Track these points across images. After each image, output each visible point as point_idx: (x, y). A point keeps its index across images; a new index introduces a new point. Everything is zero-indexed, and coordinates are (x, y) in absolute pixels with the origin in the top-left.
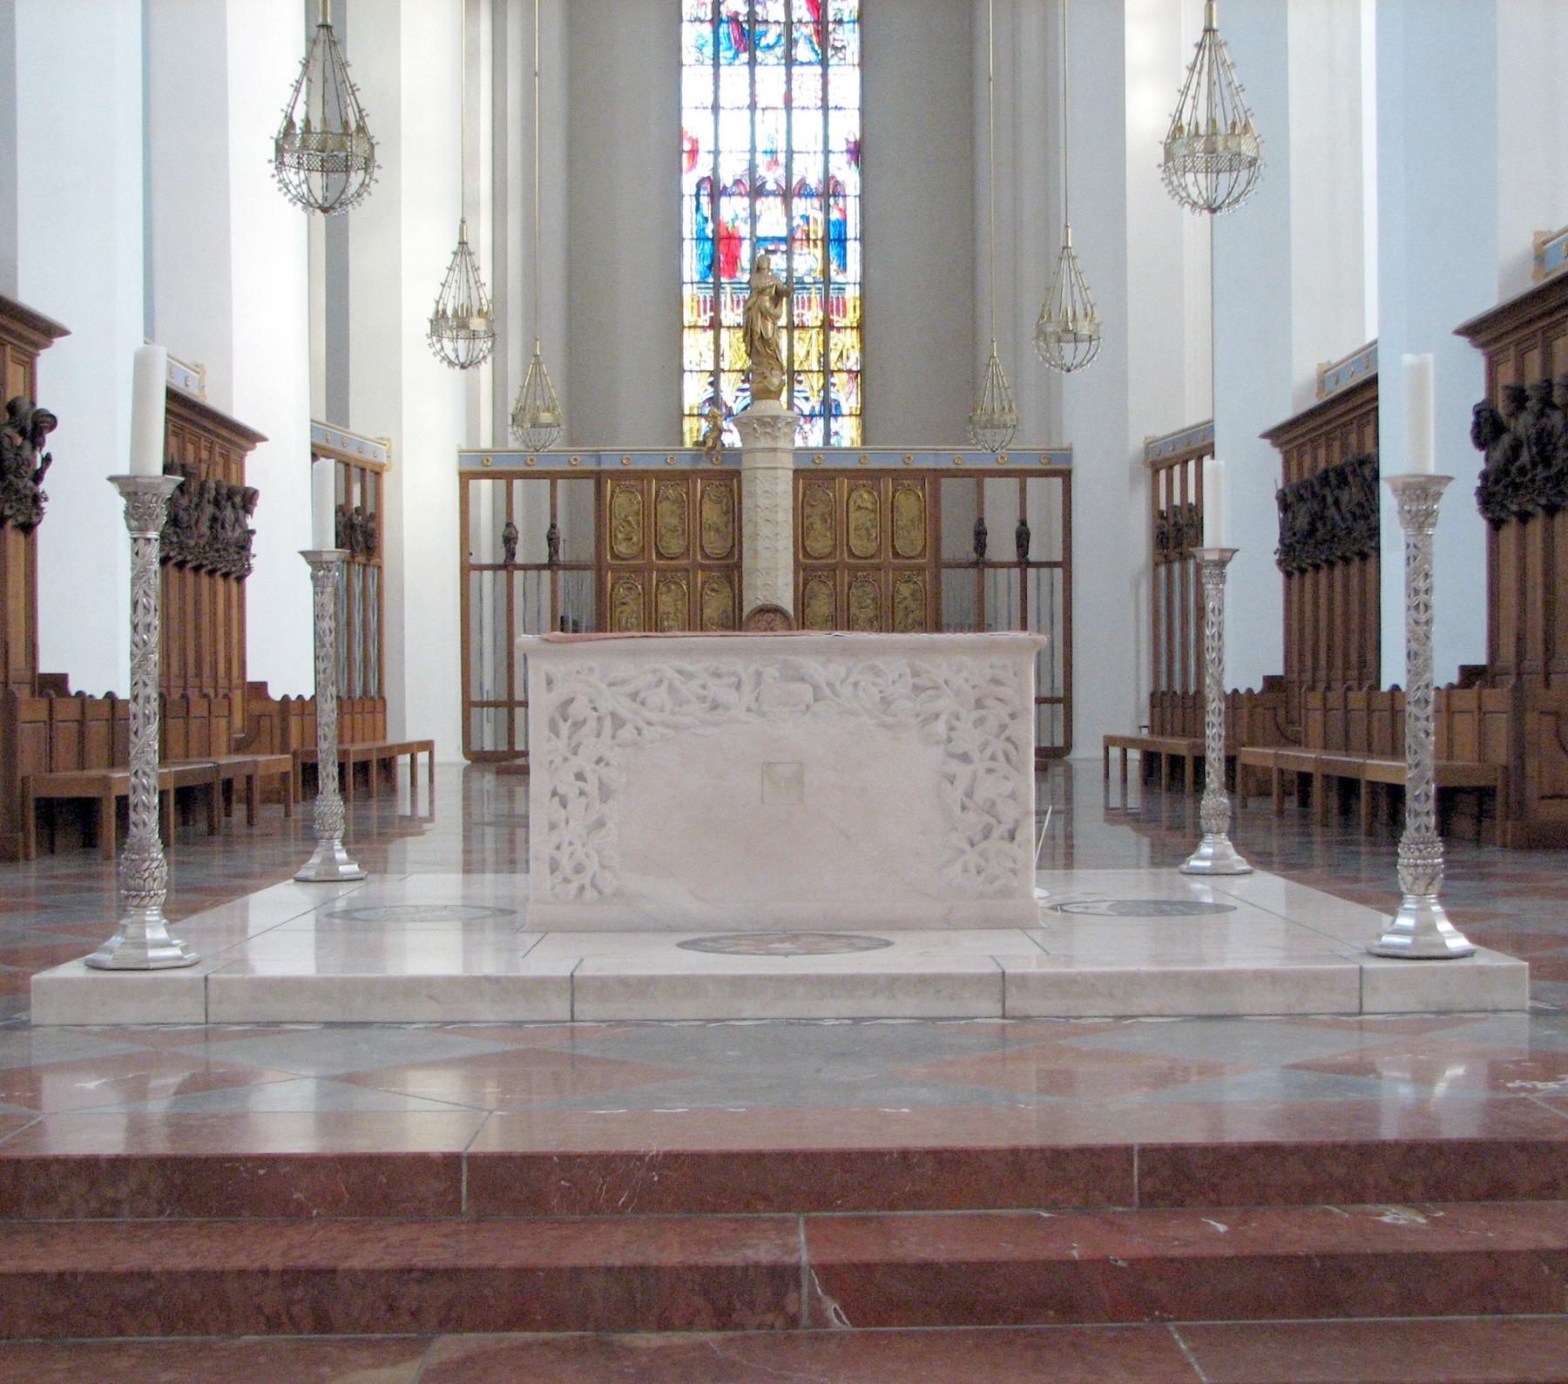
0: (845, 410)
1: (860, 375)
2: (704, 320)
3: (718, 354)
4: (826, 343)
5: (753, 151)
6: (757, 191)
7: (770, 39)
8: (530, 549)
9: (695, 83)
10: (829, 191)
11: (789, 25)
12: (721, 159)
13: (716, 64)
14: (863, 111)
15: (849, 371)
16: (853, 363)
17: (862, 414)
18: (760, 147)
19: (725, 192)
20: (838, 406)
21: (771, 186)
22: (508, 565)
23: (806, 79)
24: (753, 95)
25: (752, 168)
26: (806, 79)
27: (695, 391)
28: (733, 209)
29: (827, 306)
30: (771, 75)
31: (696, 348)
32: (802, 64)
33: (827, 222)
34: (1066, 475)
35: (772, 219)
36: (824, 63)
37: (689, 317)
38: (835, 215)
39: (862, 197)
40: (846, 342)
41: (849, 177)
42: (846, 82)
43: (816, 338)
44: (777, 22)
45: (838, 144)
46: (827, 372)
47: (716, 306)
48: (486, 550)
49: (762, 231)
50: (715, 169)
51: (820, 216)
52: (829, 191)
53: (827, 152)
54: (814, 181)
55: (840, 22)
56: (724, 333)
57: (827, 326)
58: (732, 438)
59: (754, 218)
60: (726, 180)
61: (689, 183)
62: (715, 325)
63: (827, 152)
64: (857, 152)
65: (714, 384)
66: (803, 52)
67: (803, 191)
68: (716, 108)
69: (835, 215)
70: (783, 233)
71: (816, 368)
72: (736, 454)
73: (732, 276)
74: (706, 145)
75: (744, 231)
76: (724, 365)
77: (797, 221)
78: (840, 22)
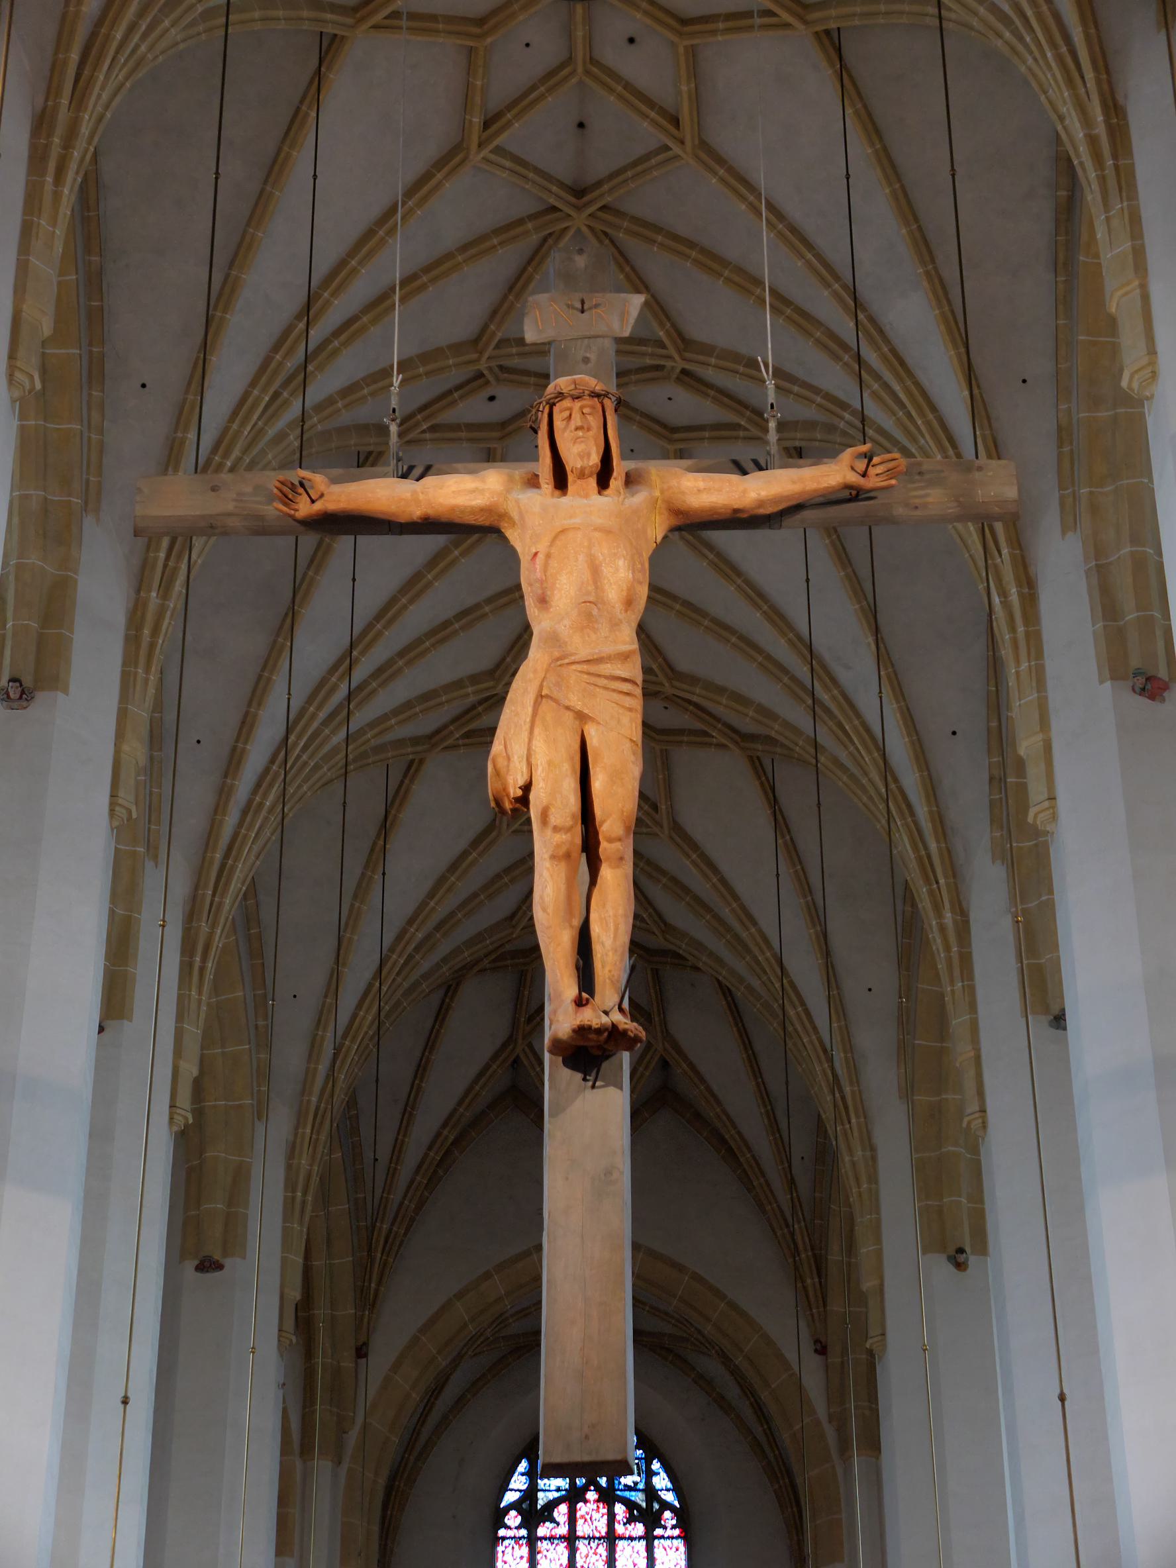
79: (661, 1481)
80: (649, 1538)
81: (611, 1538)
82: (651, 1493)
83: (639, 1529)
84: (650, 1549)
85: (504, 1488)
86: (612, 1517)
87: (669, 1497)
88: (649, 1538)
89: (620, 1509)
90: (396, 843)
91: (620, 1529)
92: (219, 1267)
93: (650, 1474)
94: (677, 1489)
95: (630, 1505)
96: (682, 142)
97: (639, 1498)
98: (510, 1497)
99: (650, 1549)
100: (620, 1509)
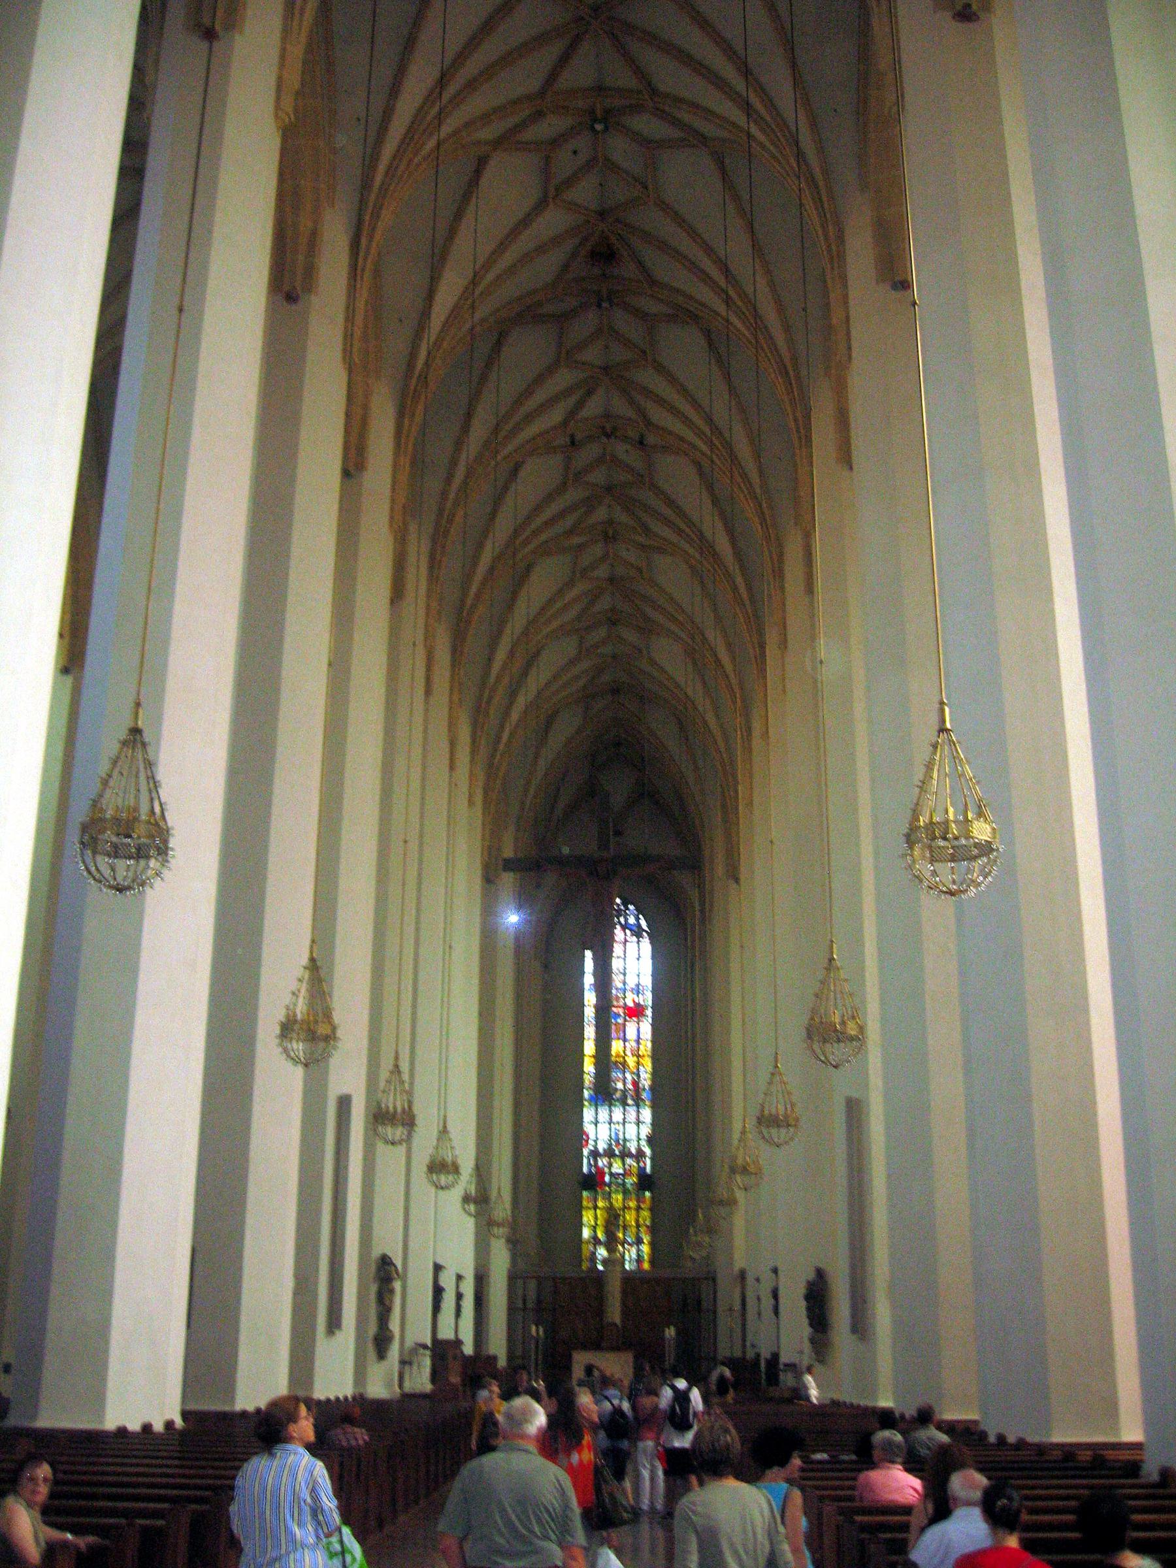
0: (645, 1241)
1: (653, 1230)
3: (596, 1218)
4: (638, 1216)
7: (618, 1095)
8: (530, 1305)
9: (588, 1114)
10: (640, 1154)
11: (624, 1091)
12: (599, 1142)
14: (652, 1124)
15: (647, 1227)
16: (648, 1223)
17: (653, 1244)
18: (613, 1137)
20: (642, 1239)
21: (617, 1152)
22: (525, 1309)
23: (632, 1112)
25: (610, 1145)
26: (632, 1112)
27: (586, 1233)
28: (602, 1162)
29: (638, 1201)
30: (618, 1114)
31: (588, 1217)
32: (628, 1105)
33: (639, 1166)
34: (714, 1280)
35: (617, 1168)
36: (638, 1106)
37: (585, 1203)
39: (652, 1159)
40: (645, 1214)
41: (647, 1151)
42: (647, 1114)
43: (633, 1212)
44: (621, 1090)
45: (643, 1136)
46: (638, 1226)
47: (595, 1200)
48: (520, 1305)
49: (614, 1170)
50: (595, 1147)
51: (635, 1164)
52: (640, 1154)
53: (639, 1139)
54: (634, 1151)
55: (644, 1089)
56: (598, 1211)
57: (638, 1209)
59: (610, 1165)
60: (601, 1151)
61: (585, 1152)
62: (595, 1207)
63: (639, 1139)
64: (650, 1140)
65: (595, 1232)
66: (630, 1102)
67: (630, 1155)
68: (596, 1123)
69: (642, 1164)
70: (621, 1171)
71: (633, 1223)
74: (592, 1136)
75: (606, 1170)
76: (599, 1223)
77: (627, 1166)
80: (638, 942)
81: (626, 941)
82: (639, 926)
83: (635, 939)
86: (625, 934)
88: (638, 942)
91: (628, 938)
93: (638, 919)
97: (635, 929)
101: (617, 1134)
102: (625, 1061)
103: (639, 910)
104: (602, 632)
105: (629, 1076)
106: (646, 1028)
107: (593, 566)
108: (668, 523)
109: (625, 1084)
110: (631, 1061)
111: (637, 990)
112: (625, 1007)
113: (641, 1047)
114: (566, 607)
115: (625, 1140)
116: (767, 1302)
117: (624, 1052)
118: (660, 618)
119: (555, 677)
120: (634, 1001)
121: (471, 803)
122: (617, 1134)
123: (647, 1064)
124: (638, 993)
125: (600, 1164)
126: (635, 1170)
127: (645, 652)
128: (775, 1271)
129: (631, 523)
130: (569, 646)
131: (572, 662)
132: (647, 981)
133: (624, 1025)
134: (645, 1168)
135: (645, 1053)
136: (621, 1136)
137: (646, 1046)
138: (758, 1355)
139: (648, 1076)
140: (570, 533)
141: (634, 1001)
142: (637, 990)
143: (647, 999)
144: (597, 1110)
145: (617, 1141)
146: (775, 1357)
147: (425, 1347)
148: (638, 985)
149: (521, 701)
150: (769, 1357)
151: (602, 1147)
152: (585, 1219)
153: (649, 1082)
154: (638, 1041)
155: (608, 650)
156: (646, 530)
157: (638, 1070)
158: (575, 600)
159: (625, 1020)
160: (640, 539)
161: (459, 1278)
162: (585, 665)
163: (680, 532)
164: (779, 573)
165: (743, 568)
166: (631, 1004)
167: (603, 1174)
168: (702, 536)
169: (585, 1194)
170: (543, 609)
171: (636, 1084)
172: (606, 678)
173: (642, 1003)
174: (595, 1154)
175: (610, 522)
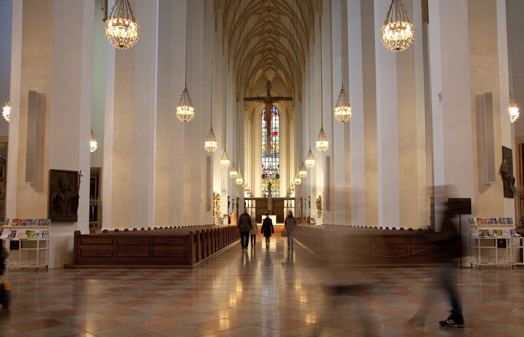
2: (264, 182)
5: (269, 166)
6: (270, 170)
8: (250, 206)
12: (266, 167)
13: (265, 158)
19: (266, 170)
21: (270, 169)
23: (274, 159)
24: (269, 161)
25: (269, 167)
26: (274, 159)
28: (267, 171)
35: (271, 173)
38: (277, 172)
45: (277, 165)
50: (265, 168)
52: (277, 170)
55: (277, 153)
58: (267, 197)
59: (269, 172)
64: (279, 166)
67: (273, 170)
68: (265, 162)
70: (271, 174)
72: (267, 198)
73: (267, 178)
74: (264, 165)
75: (268, 174)
78: (277, 153)
79: (277, 111)
80: (276, 116)
82: (276, 112)
83: (275, 115)
84: (276, 117)
85: (263, 111)
87: (277, 112)
88: (276, 116)
89: (273, 113)
90: (253, 62)
92: (238, 101)
94: (278, 112)
95: (274, 113)
96: (278, 22)
97: (275, 112)
98: (263, 112)
99: (276, 117)
100: (273, 113)
101: (270, 165)
102: (272, 146)
103: (276, 108)
104: (267, 35)
105: (273, 150)
106: (278, 138)
107: (264, 18)
108: (284, 7)
109: (272, 152)
110: (274, 146)
111: (275, 128)
112: (272, 132)
113: (277, 143)
114: (258, 29)
115: (273, 166)
116: (308, 205)
117: (272, 144)
118: (280, 31)
119: (255, 47)
120: (274, 131)
121: (233, 82)
122: (270, 165)
123: (278, 147)
124: (276, 130)
125: (266, 172)
126: (275, 174)
127: (278, 41)
128: (310, 197)
129: (274, 6)
130: (258, 39)
131: (259, 43)
132: (278, 126)
133: (272, 136)
134: (277, 173)
135: (277, 144)
136: (271, 165)
137: (277, 143)
138: (305, 217)
139: (278, 150)
140: (258, 10)
141: (274, 131)
142: (275, 128)
143: (278, 130)
144: (265, 159)
145: (271, 166)
146: (309, 217)
147: (226, 215)
148: (276, 127)
149: (246, 53)
150: (308, 217)
151: (266, 168)
152: (263, 186)
153: (278, 151)
154: (276, 141)
155: (268, 40)
156: (279, 9)
157: (276, 148)
158: (260, 27)
159: (272, 136)
160: (278, 11)
161: (233, 200)
162: (262, 44)
163: (287, 10)
164: (313, 24)
165: (304, 20)
166: (273, 132)
167: (267, 175)
168: (293, 12)
169: (263, 179)
170: (252, 29)
171: (275, 152)
172: (267, 47)
173: (276, 131)
174: (264, 169)
175: (269, 6)
